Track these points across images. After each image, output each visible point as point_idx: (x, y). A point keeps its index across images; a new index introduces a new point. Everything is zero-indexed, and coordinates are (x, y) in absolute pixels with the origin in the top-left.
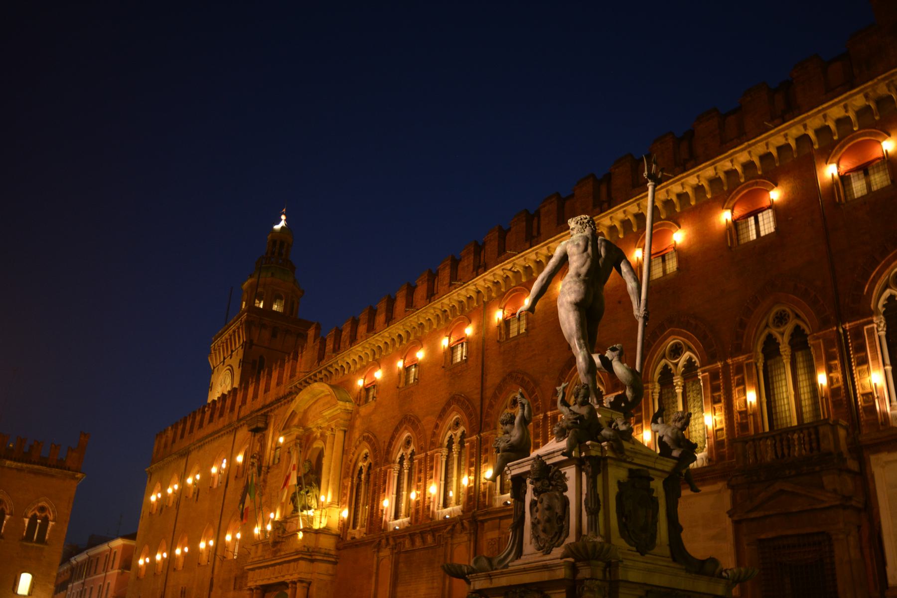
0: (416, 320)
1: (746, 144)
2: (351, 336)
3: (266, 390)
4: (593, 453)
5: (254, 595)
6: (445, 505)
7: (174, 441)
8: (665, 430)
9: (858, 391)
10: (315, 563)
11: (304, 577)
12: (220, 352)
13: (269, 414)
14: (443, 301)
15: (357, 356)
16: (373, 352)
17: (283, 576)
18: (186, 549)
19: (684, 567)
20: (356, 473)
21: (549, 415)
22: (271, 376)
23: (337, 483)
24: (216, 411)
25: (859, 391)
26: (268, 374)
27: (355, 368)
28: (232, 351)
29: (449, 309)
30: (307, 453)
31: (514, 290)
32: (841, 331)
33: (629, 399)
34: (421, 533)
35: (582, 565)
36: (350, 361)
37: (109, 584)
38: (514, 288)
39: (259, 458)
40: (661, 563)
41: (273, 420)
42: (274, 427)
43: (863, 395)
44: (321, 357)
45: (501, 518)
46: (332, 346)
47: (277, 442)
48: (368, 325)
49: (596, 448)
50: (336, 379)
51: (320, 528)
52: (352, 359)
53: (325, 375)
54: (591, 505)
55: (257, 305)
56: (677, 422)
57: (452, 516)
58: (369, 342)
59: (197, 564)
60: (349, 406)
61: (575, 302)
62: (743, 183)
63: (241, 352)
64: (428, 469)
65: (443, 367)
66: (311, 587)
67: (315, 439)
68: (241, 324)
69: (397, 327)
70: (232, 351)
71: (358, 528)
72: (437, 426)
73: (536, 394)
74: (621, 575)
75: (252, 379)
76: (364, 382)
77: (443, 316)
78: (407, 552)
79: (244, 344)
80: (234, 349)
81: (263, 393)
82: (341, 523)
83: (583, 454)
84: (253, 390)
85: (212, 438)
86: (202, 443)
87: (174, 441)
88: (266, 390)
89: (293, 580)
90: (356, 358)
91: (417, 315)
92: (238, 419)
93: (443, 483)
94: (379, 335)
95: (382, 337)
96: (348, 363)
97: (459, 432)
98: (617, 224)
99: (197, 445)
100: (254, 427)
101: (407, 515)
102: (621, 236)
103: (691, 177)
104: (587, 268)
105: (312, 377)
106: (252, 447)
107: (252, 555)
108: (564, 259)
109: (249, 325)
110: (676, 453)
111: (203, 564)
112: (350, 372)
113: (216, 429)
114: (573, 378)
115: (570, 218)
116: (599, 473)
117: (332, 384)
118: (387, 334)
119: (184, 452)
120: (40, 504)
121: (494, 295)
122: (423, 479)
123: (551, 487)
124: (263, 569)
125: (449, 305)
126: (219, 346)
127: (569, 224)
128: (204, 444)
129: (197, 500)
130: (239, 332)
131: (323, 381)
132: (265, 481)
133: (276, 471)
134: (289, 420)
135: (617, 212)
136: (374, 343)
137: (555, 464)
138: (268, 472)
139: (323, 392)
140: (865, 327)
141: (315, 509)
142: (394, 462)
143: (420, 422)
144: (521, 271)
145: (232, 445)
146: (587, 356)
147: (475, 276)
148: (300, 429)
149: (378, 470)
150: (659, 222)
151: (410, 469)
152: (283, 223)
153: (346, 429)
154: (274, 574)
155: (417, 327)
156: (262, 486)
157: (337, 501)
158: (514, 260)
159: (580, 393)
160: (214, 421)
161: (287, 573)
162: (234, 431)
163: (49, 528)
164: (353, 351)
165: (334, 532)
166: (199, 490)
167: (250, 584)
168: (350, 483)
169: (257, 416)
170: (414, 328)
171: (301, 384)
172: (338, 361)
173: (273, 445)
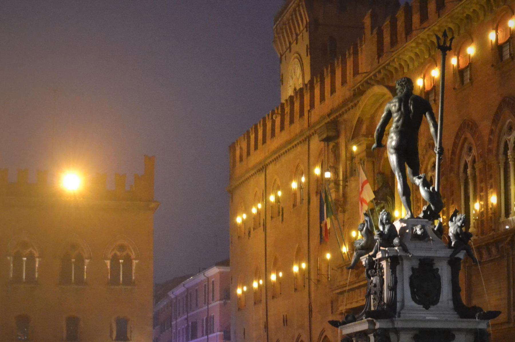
2: (405, 27)
12: (284, 37)
18: (281, 274)
28: (297, 35)
36: (406, 58)
41: (343, 126)
47: (352, 152)
57: (512, 227)
63: (306, 35)
64: (488, 178)
65: (492, 66)
70: (297, 35)
79: (308, 26)
80: (298, 33)
81: (330, 95)
84: (329, 81)
85: (286, 149)
87: (248, 154)
88: (333, 91)
90: (413, 55)
92: (309, 126)
94: (429, 29)
96: (405, 61)
100: (324, 136)
105: (373, 78)
122: (484, 189)
126: (282, 29)
129: (282, 220)
130: (299, 11)
132: (344, 195)
160: (285, 128)
164: (408, 47)
167: (340, 308)
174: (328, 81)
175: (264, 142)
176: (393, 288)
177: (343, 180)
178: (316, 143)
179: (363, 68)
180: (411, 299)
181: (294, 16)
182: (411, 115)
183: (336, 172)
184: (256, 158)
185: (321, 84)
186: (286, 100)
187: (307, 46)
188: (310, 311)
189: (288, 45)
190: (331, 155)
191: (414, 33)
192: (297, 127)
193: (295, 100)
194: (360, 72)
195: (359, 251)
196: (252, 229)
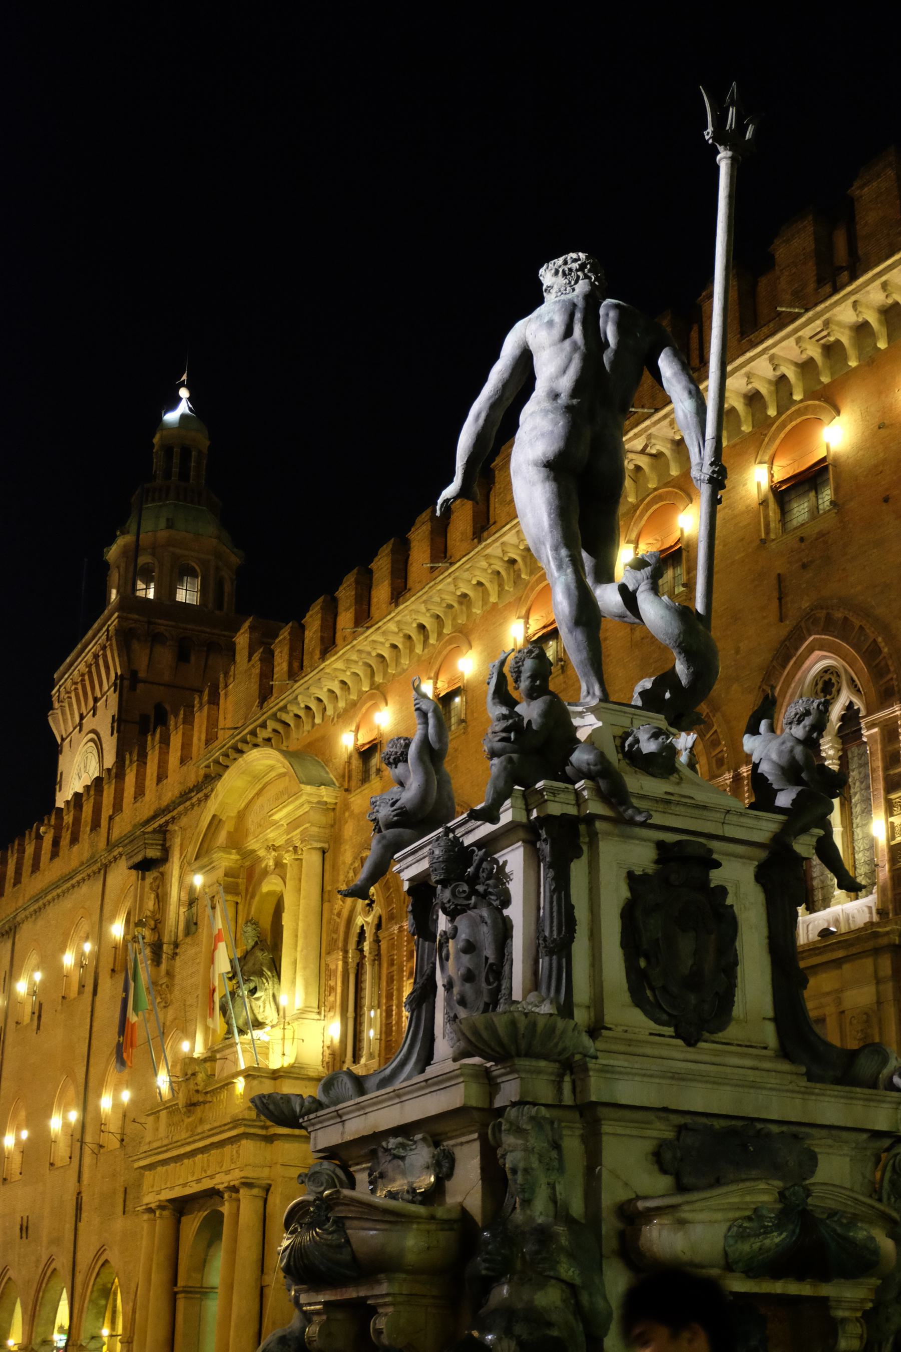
0: (452, 588)
2: (322, 639)
3: (161, 777)
4: (555, 809)
5: (158, 1221)
8: (766, 746)
10: (276, 1143)
11: (255, 1175)
12: (70, 705)
13: (170, 827)
14: (505, 539)
15: (337, 683)
16: (369, 670)
17: (212, 1177)
19: (803, 1069)
20: (353, 940)
21: (745, 774)
23: (314, 966)
24: (64, 831)
27: (335, 708)
28: (96, 700)
29: (518, 555)
30: (250, 905)
31: (655, 496)
33: (684, 681)
35: (503, 1071)
38: (656, 493)
39: (156, 927)
40: (735, 1061)
41: (178, 841)
42: (181, 855)
44: (265, 694)
46: (285, 666)
47: (192, 889)
48: (356, 610)
49: (562, 797)
50: (298, 738)
51: (282, 1067)
52: (325, 689)
53: (275, 731)
54: (551, 931)
55: (141, 594)
56: (794, 726)
58: (359, 648)
59: (48, 1165)
60: (327, 794)
61: (545, 460)
63: (113, 698)
66: (271, 1198)
67: (265, 873)
68: (108, 639)
69: (413, 607)
70: (96, 700)
71: (363, 1061)
73: (715, 728)
74: (597, 1090)
75: (131, 754)
76: (356, 739)
77: (509, 574)
80: (99, 696)
82: (327, 1052)
83: (535, 814)
85: (59, 891)
86: (41, 903)
88: (161, 777)
89: (232, 1183)
90: (336, 687)
91: (453, 576)
95: (384, 633)
96: (319, 700)
99: (32, 909)
100: (138, 858)
102: (882, 345)
104: (574, 378)
106: (140, 901)
107: (149, 1136)
108: (525, 359)
110: (784, 799)
111: (59, 1164)
112: (325, 720)
113: (66, 870)
114: (793, 685)
115: (542, 266)
116: (578, 854)
117: (292, 748)
118: (392, 627)
119: (7, 927)
123: (473, 899)
124: (172, 1165)
125: (517, 547)
127: (541, 278)
128: (45, 905)
129: (38, 1028)
131: (272, 746)
132: (170, 974)
133: (192, 951)
134: (210, 835)
135: (869, 288)
136: (368, 649)
137: (479, 844)
138: (176, 954)
139: (272, 768)
141: (273, 1026)
144: (667, 452)
145: (99, 903)
146: (573, 586)
148: (230, 854)
149: (396, 928)
152: (184, 407)
153: (326, 846)
154: (193, 1174)
155: (455, 605)
156: (164, 986)
157: (316, 1005)
158: (647, 428)
159: (522, 669)
161: (218, 1170)
162: (102, 872)
164: (327, 671)
165: (312, 1074)
166: (41, 1005)
167: (146, 1200)
168: (340, 963)
169: (144, 833)
170: (450, 607)
171: (226, 755)
172: (296, 698)
173: (183, 894)
180: (626, 997)
181: (94, 669)
182: (607, 357)
187: (113, 717)
193: (84, 799)
195: (389, 833)
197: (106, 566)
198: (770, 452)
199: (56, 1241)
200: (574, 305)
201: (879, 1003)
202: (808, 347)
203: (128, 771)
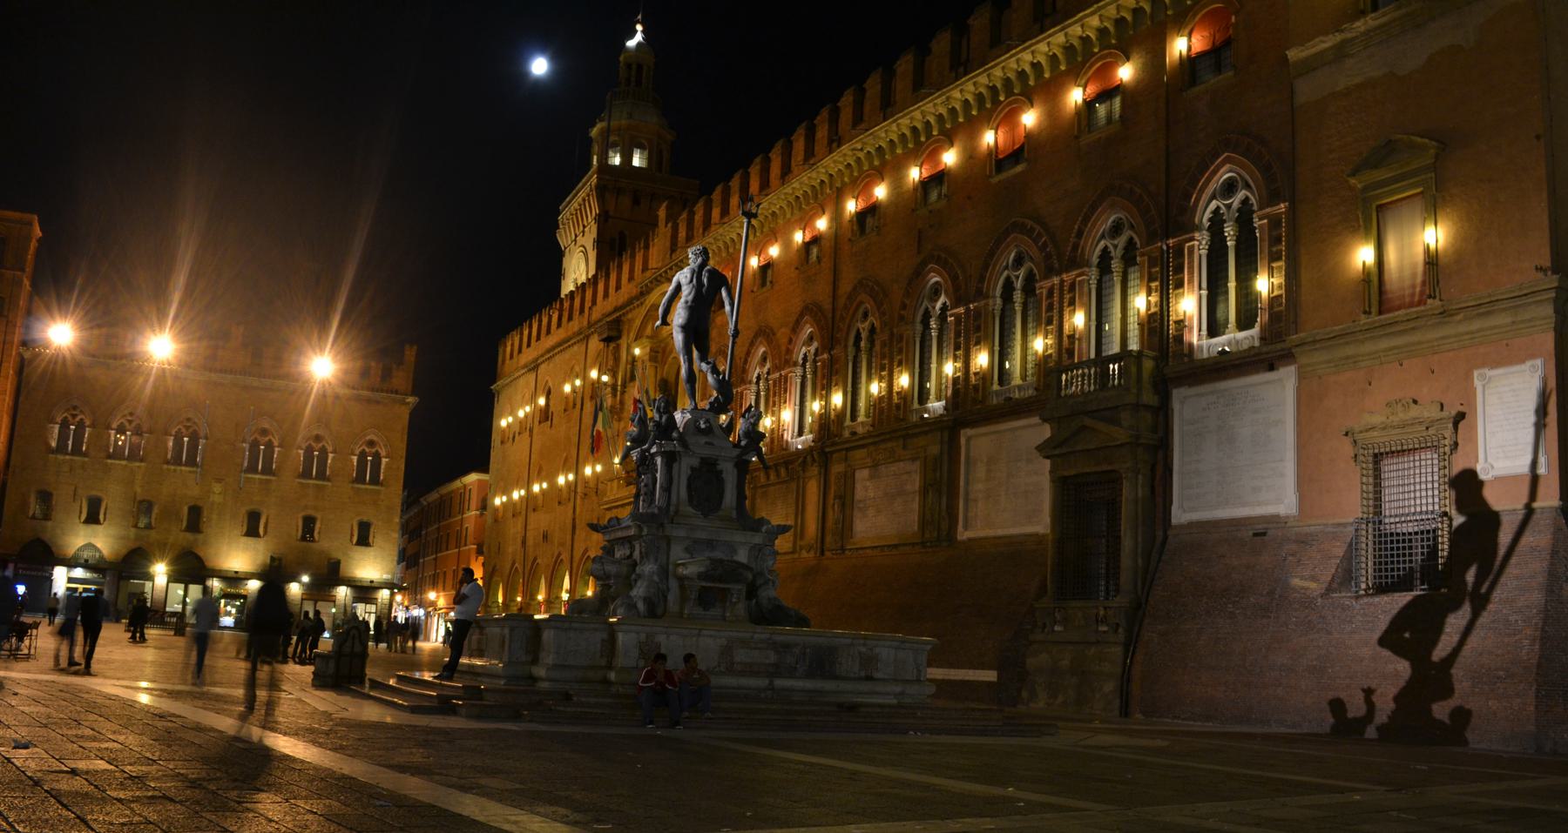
1: (1095, 6)
2: (704, 221)
3: (618, 288)
4: (668, 449)
6: (800, 433)
7: (512, 357)
9: (1171, 318)
12: (569, 227)
13: (622, 318)
22: (609, 278)
25: (1173, 318)
26: (618, 267)
28: (584, 227)
30: (663, 369)
32: (1165, 247)
34: (784, 462)
37: (467, 528)
43: (1176, 322)
45: (847, 450)
62: (1097, 53)
65: (797, 268)
68: (591, 190)
70: (584, 227)
72: (790, 341)
78: (762, 486)
85: (562, 348)
87: (520, 351)
88: (618, 288)
93: (797, 408)
97: (812, 349)
98: (970, 98)
100: (605, 336)
101: (811, 432)
103: (1041, 44)
105: (663, 275)
109: (601, 191)
120: (368, 438)
121: (846, 179)
140: (1187, 245)
142: (750, 382)
143: (774, 334)
147: (881, 120)
150: (1013, 98)
151: (768, 390)
152: (639, 37)
160: (563, 325)
163: (383, 466)
174: (613, 277)
175: (538, 339)
176: (667, 489)
177: (621, 386)
178: (595, 343)
179: (653, 263)
182: (704, 290)
183: (614, 375)
184: (528, 355)
185: (605, 280)
186: (566, 295)
188: (574, 527)
189: (574, 237)
190: (611, 357)
191: (713, 228)
192: (575, 325)
194: (650, 267)
196: (517, 435)
197: (591, 140)
198: (921, 160)
199: (562, 544)
200: (694, 270)
201: (941, 453)
202: (940, 108)
203: (599, 281)
